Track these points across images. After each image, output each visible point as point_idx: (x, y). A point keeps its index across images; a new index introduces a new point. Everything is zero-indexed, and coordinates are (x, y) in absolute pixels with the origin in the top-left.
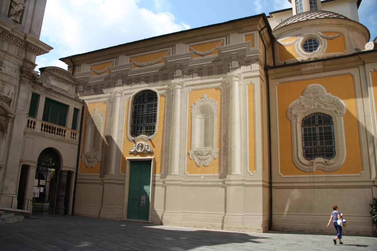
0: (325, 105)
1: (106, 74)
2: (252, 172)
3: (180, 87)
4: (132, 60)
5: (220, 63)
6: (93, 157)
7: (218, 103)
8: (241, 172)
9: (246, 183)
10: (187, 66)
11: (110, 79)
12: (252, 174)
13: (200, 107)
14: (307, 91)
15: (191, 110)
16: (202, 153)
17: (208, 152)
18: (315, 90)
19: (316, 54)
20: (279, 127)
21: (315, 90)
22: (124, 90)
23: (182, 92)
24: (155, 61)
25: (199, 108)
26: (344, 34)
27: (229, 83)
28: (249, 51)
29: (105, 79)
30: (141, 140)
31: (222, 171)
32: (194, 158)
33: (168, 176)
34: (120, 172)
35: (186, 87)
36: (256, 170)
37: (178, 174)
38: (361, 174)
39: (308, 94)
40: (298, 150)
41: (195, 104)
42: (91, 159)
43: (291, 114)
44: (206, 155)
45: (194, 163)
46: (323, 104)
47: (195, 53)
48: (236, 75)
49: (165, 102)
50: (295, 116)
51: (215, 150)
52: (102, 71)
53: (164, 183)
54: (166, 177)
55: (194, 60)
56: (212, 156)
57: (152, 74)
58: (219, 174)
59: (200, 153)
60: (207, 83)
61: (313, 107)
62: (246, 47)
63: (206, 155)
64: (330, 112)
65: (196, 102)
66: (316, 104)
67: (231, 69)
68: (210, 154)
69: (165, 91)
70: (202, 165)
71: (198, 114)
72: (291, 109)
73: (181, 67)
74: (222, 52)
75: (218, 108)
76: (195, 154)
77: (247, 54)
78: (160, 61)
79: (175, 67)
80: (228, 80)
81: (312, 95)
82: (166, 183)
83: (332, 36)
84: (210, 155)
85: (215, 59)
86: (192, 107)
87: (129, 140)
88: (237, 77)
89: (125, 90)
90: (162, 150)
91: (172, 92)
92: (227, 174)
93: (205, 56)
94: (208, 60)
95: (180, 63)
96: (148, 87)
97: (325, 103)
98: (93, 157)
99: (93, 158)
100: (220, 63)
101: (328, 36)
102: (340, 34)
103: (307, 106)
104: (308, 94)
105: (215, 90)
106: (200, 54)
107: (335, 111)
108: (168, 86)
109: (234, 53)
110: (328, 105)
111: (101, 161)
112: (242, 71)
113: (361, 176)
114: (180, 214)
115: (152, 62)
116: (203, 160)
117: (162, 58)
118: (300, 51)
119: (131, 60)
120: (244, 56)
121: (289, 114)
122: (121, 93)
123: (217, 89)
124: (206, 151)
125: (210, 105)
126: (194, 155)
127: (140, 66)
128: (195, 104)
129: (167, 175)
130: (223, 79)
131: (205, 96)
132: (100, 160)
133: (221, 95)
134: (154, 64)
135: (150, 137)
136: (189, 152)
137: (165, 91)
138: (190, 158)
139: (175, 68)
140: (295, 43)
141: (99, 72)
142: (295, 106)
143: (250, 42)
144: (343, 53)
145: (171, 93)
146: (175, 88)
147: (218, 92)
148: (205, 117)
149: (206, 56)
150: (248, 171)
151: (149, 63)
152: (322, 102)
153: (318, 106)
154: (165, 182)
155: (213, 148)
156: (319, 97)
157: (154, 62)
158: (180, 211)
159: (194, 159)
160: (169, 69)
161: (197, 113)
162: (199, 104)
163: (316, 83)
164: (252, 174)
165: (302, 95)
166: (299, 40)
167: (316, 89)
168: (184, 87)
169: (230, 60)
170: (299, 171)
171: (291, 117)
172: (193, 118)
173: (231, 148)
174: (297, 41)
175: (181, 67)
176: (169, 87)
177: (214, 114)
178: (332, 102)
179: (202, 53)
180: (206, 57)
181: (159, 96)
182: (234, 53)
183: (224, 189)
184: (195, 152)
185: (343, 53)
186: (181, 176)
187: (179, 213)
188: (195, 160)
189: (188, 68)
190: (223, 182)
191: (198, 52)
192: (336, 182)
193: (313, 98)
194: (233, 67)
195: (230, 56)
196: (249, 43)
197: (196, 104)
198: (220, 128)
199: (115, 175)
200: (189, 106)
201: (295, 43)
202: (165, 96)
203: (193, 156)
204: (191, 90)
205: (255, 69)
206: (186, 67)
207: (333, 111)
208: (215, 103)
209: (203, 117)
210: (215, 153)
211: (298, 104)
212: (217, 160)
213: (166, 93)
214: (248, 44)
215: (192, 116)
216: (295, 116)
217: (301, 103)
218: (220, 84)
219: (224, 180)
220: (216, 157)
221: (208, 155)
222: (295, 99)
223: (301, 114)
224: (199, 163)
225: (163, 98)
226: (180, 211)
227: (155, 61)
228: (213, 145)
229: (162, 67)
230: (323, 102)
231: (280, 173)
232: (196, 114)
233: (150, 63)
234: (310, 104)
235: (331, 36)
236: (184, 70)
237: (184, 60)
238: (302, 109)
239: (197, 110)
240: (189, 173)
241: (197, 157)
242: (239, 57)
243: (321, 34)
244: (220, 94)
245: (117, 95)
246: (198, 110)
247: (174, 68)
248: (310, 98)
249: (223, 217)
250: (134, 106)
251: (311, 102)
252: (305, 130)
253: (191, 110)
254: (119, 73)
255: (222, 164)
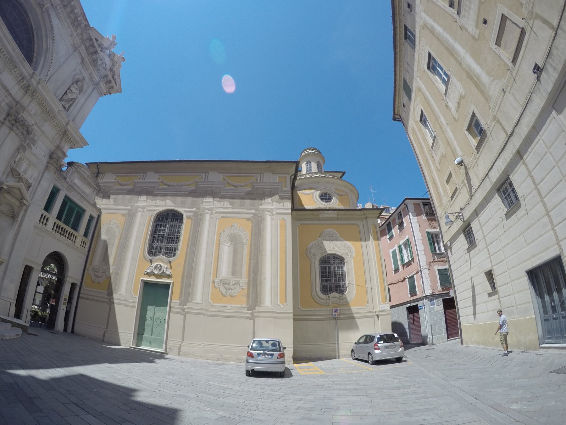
3: (209, 212)
7: (249, 234)
9: (276, 316)
13: (229, 235)
14: (324, 235)
17: (235, 282)
23: (210, 218)
25: (228, 236)
27: (261, 216)
30: (159, 261)
33: (188, 304)
35: (216, 213)
36: (287, 303)
37: (201, 302)
43: (311, 253)
44: (234, 285)
45: (220, 292)
47: (229, 183)
49: (191, 224)
50: (314, 255)
51: (244, 279)
53: (184, 310)
54: (186, 305)
56: (240, 286)
59: (227, 282)
63: (234, 285)
64: (343, 254)
65: (226, 230)
66: (332, 246)
68: (238, 284)
70: (228, 294)
74: (255, 187)
76: (221, 282)
78: (191, 184)
82: (185, 311)
84: (238, 285)
86: (220, 234)
87: (146, 259)
89: (148, 206)
90: (183, 275)
92: (256, 306)
93: (238, 187)
96: (175, 207)
107: (347, 254)
122: (143, 208)
123: (248, 219)
124: (233, 280)
125: (240, 235)
126: (220, 283)
127: (168, 186)
128: (224, 231)
129: (187, 302)
130: (255, 211)
135: (170, 259)
137: (193, 214)
138: (215, 286)
140: (314, 193)
143: (283, 183)
145: (199, 217)
147: (250, 223)
150: (279, 303)
153: (333, 248)
154: (184, 310)
155: (241, 278)
159: (219, 288)
161: (225, 241)
167: (331, 233)
168: (213, 213)
172: (221, 245)
176: (197, 211)
177: (244, 243)
179: (236, 184)
181: (185, 217)
183: (252, 321)
184: (221, 280)
188: (221, 289)
189: (219, 195)
191: (230, 182)
197: (226, 231)
198: (250, 259)
202: (192, 219)
204: (220, 217)
205: (287, 207)
209: (232, 246)
213: (193, 215)
214: (282, 184)
216: (314, 255)
217: (319, 244)
218: (252, 215)
220: (244, 288)
221: (236, 285)
223: (319, 254)
224: (226, 293)
225: (190, 220)
228: (241, 275)
239: (226, 238)
241: (224, 286)
245: (138, 210)
246: (227, 238)
250: (155, 223)
252: (322, 268)
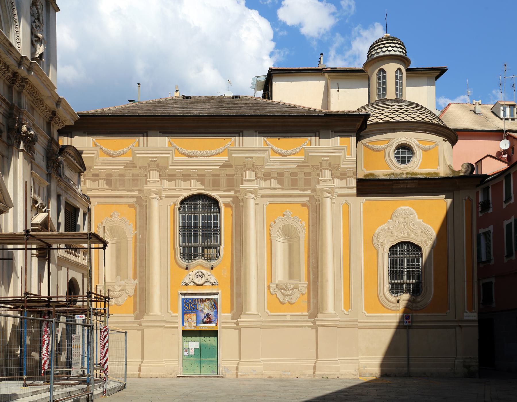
0: (415, 233)
1: (128, 159)
2: (347, 310)
4: (172, 142)
5: (307, 170)
6: (118, 289)
7: (305, 224)
8: (335, 311)
10: (262, 166)
11: (135, 168)
12: (346, 313)
14: (396, 215)
15: (270, 230)
16: (286, 287)
17: (294, 286)
18: (406, 214)
19: (409, 168)
20: (364, 256)
21: (406, 214)
22: (164, 189)
23: (256, 204)
24: (212, 151)
25: (280, 228)
26: (439, 145)
28: (345, 160)
29: (125, 167)
30: (199, 267)
31: (312, 308)
32: (276, 293)
33: (242, 316)
34: (169, 311)
35: (262, 197)
36: (351, 309)
37: (256, 313)
38: (446, 314)
39: (398, 218)
40: (385, 285)
41: (275, 222)
42: (116, 292)
43: (378, 241)
44: (292, 289)
45: (277, 299)
46: (413, 232)
47: (273, 150)
48: (329, 190)
49: (232, 215)
50: (383, 244)
52: (118, 152)
54: (239, 317)
55: (272, 160)
57: (209, 171)
58: (308, 312)
59: (284, 286)
60: (290, 196)
61: (402, 235)
62: (341, 154)
63: (292, 289)
64: (420, 242)
65: (277, 221)
67: (321, 180)
68: (296, 288)
69: (231, 199)
70: (286, 301)
71: (279, 236)
72: (378, 235)
73: (253, 168)
74: (310, 155)
75: (306, 231)
76: (277, 287)
77: (342, 163)
79: (245, 165)
80: (318, 195)
81: (402, 220)
83: (428, 146)
84: (297, 290)
85: (300, 162)
86: (270, 226)
87: (180, 266)
88: (329, 193)
91: (241, 201)
92: (318, 313)
93: (286, 156)
94: (291, 162)
95: (252, 161)
96: (205, 190)
97: (415, 231)
98: (118, 289)
99: (120, 291)
100: (307, 170)
101: (424, 146)
102: (435, 144)
103: (396, 232)
104: (398, 218)
105: (301, 206)
106: (280, 152)
107: (425, 242)
108: (236, 192)
109: (326, 159)
110: (419, 234)
111: (135, 295)
112: (335, 186)
113: (447, 316)
114: (262, 363)
115: (208, 151)
116: (288, 296)
117: (224, 149)
118: (392, 161)
119: (171, 143)
120: (339, 166)
121: (375, 241)
124: (291, 284)
125: (295, 226)
127: (188, 156)
128: (275, 222)
129: (241, 314)
130: (312, 193)
131: (288, 213)
132: (131, 294)
133: (309, 214)
134: (210, 156)
135: (213, 263)
136: (269, 285)
137: (231, 199)
139: (244, 168)
140: (386, 148)
141: (112, 152)
142: (383, 231)
143: (346, 147)
144: (436, 170)
145: (241, 204)
146: (246, 196)
148: (289, 241)
149: (288, 157)
150: (343, 309)
151: (203, 152)
152: (413, 230)
153: (408, 234)
154: (239, 323)
155: (300, 282)
156: (410, 223)
157: (211, 152)
158: (261, 359)
159: (276, 294)
160: (235, 168)
161: (277, 235)
162: (280, 223)
163: (408, 206)
164: (346, 313)
165: (391, 219)
166: (391, 145)
167: (406, 212)
168: (258, 198)
169: (320, 169)
170: (385, 309)
171: (378, 245)
172: (272, 240)
173: (322, 282)
174: (389, 146)
175: (253, 168)
177: (301, 238)
178: (422, 231)
179: (283, 151)
180: (288, 158)
181: (221, 205)
182: (326, 159)
184: (277, 285)
185: (436, 170)
186: (260, 315)
187: (260, 361)
188: (278, 296)
189: (263, 170)
190: (314, 323)
191: (277, 149)
192: (422, 322)
193: (403, 224)
194: (324, 178)
195: (320, 162)
196: (345, 148)
197: (277, 222)
198: (309, 257)
199: (162, 315)
200: (267, 225)
201: (386, 148)
203: (275, 291)
204: (268, 203)
205: (351, 186)
206: (260, 168)
207: (423, 241)
208: (302, 224)
209: (286, 241)
210: (303, 287)
211: (386, 230)
212: (306, 296)
214: (344, 149)
215: (272, 238)
216: (383, 244)
217: (389, 229)
218: (308, 199)
219: (314, 320)
220: (304, 292)
221: (294, 290)
222: (383, 223)
224: (283, 299)
226: (261, 359)
227: (212, 151)
229: (224, 163)
230: (414, 230)
231: (364, 311)
232: (277, 236)
233: (204, 153)
234: (398, 231)
235: (426, 147)
236: (257, 172)
237: (258, 157)
238: (390, 235)
239: (278, 231)
240: (271, 312)
241: (280, 291)
242: (331, 166)
243: (417, 143)
244: (307, 213)
246: (280, 230)
247: (243, 167)
248: (400, 223)
249: (315, 364)
251: (400, 229)
252: (392, 261)
253: (270, 230)
254: (152, 161)
255: (312, 301)
